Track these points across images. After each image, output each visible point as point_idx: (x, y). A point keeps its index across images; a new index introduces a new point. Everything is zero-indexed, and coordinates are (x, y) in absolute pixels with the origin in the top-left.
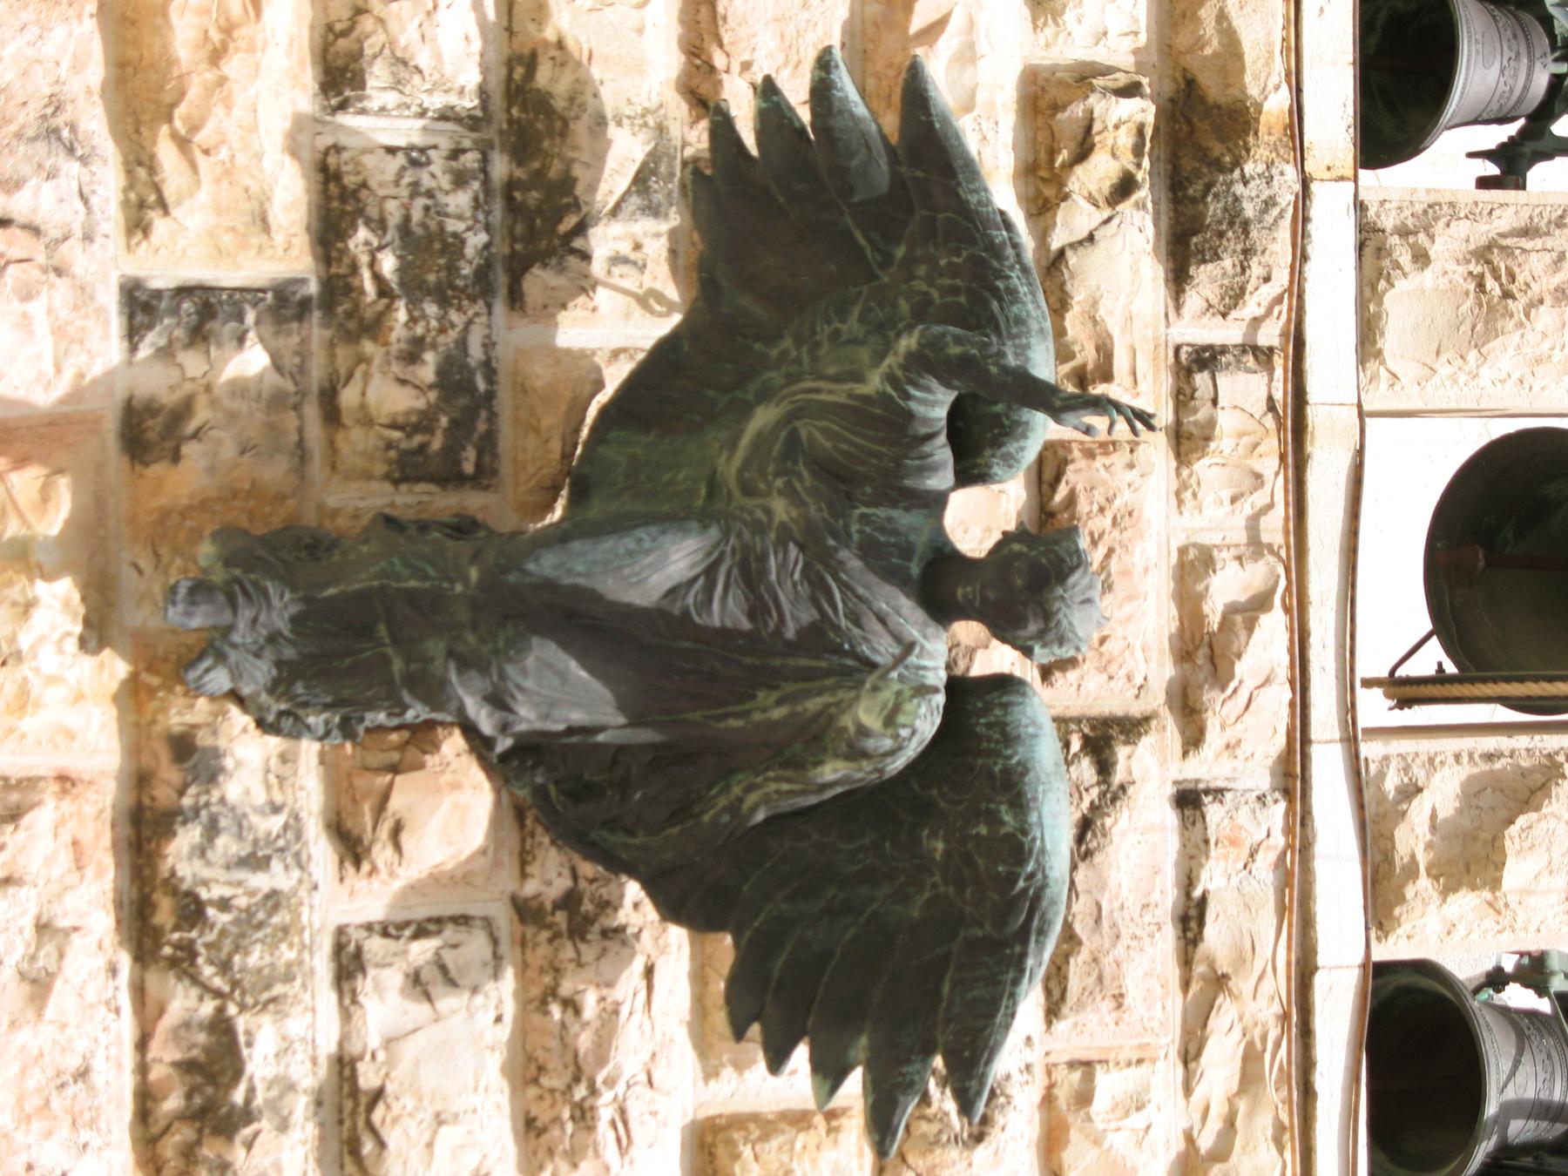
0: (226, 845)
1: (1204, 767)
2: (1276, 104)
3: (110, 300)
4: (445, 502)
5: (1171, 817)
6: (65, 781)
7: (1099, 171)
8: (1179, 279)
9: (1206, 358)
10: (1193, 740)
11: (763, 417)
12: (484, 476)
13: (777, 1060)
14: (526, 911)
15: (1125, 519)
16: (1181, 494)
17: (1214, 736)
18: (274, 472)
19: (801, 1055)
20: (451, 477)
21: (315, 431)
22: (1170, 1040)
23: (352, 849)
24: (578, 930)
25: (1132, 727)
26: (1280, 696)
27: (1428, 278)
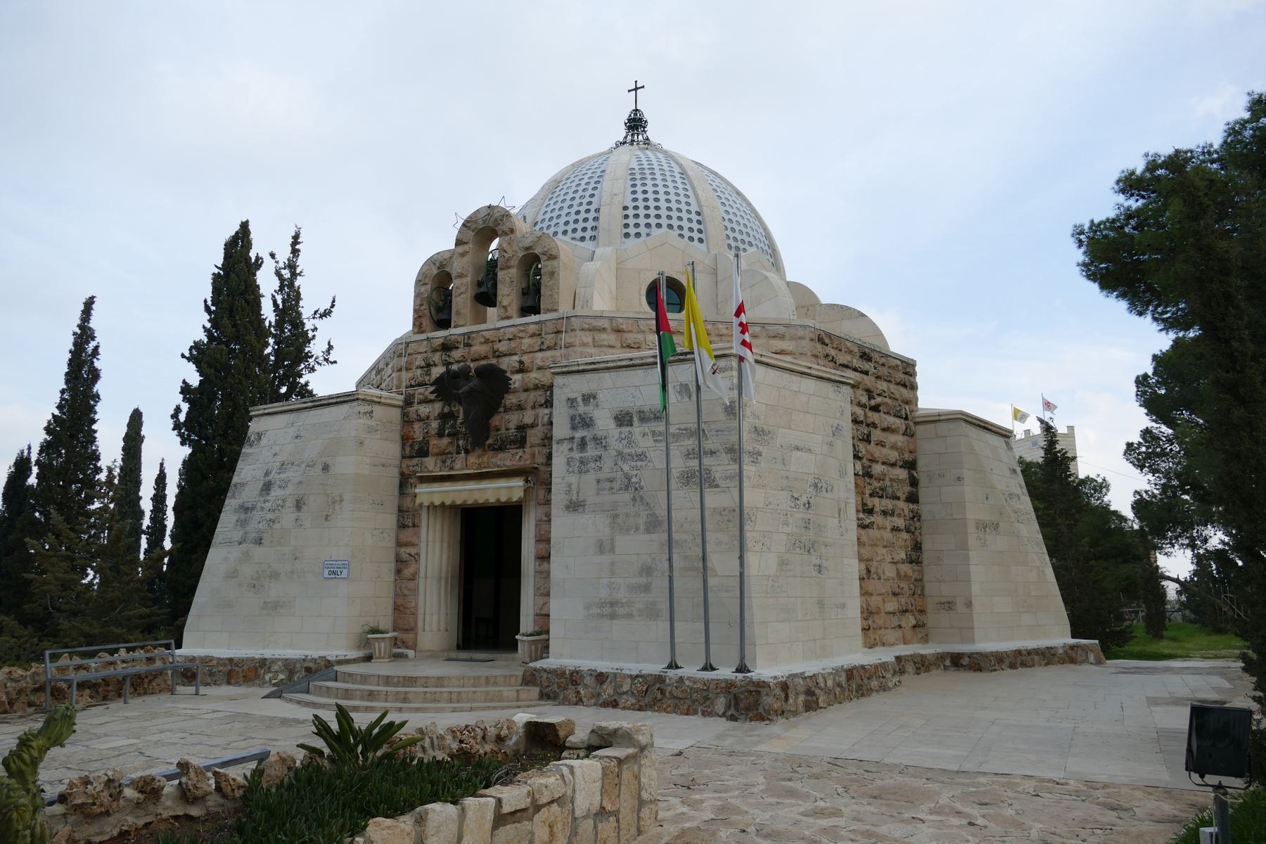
2: (442, 340)
7: (447, 358)
8: (458, 348)
23: (498, 430)
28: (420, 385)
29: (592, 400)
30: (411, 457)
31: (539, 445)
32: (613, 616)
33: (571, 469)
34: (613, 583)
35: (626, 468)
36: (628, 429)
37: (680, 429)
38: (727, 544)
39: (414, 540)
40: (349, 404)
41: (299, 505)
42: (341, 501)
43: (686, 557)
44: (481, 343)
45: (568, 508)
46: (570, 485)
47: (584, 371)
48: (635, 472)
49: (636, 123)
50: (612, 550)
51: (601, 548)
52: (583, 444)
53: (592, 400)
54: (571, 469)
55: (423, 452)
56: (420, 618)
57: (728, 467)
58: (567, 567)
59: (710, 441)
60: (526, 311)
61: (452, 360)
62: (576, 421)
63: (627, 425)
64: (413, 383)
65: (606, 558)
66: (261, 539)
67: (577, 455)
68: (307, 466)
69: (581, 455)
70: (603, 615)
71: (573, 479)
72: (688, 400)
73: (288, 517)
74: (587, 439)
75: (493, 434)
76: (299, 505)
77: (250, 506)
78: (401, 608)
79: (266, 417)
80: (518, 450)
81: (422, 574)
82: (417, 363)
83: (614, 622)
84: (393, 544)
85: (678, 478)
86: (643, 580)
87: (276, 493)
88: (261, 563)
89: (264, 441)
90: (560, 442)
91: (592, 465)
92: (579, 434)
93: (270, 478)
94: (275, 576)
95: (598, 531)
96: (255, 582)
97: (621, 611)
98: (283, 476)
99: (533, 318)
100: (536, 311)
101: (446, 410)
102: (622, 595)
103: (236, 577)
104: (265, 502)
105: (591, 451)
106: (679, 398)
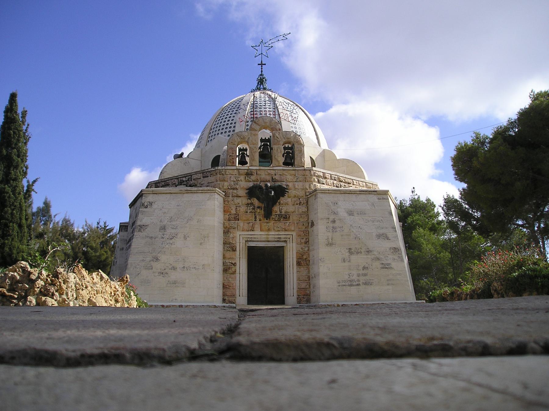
0: (276, 218)
1: (274, 175)
2: (246, 171)
3: (255, 221)
4: (263, 208)
5: (276, 176)
6: (273, 224)
7: (249, 179)
8: (253, 175)
9: (257, 174)
10: (273, 175)
11: (260, 196)
12: (262, 206)
13: (285, 196)
14: (279, 205)
15: (264, 178)
16: (263, 175)
17: (273, 174)
18: (261, 215)
19: (285, 195)
20: (262, 208)
21: (260, 213)
22: (286, 176)
23: (276, 212)
24: (280, 203)
25: (272, 178)
26: (271, 171)
27: (253, 163)
28: (234, 189)
29: (336, 204)
30: (229, 220)
31: (297, 220)
32: (351, 285)
33: (328, 230)
34: (351, 273)
35: (354, 231)
36: (353, 217)
37: (373, 219)
38: (397, 260)
39: (234, 256)
40: (209, 193)
41: (185, 238)
42: (208, 237)
43: (383, 264)
44: (266, 175)
45: (327, 245)
46: (328, 237)
47: (330, 193)
48: (358, 233)
49: (261, 81)
50: (349, 261)
51: (344, 261)
52: (334, 221)
53: (336, 204)
54: (328, 230)
55: (236, 218)
56: (238, 290)
57: (393, 233)
58: (328, 267)
59: (385, 224)
60: (285, 164)
61: (251, 180)
62: (330, 212)
63: (352, 215)
64: (230, 188)
65: (346, 264)
66: (165, 252)
67: (331, 225)
68: (188, 220)
69: (333, 225)
70: (346, 285)
71: (330, 234)
72: (374, 208)
73: (179, 243)
74: (335, 219)
75: (274, 213)
76: (185, 238)
77: (153, 236)
78: (228, 287)
79: (153, 195)
80: (286, 221)
81: (238, 271)
82: (232, 179)
83: (352, 287)
84: (221, 257)
85: (375, 236)
86: (365, 272)
87: (169, 231)
88: (165, 263)
89: (155, 206)
90: (321, 219)
91: (339, 229)
92: (332, 217)
93: (165, 223)
94: (174, 268)
95: (343, 254)
96: (162, 271)
97: (355, 283)
98: (173, 223)
99: (290, 168)
100: (292, 164)
101: (249, 201)
102: (355, 277)
103: (152, 269)
104: (163, 235)
105: (337, 224)
106: (371, 207)
